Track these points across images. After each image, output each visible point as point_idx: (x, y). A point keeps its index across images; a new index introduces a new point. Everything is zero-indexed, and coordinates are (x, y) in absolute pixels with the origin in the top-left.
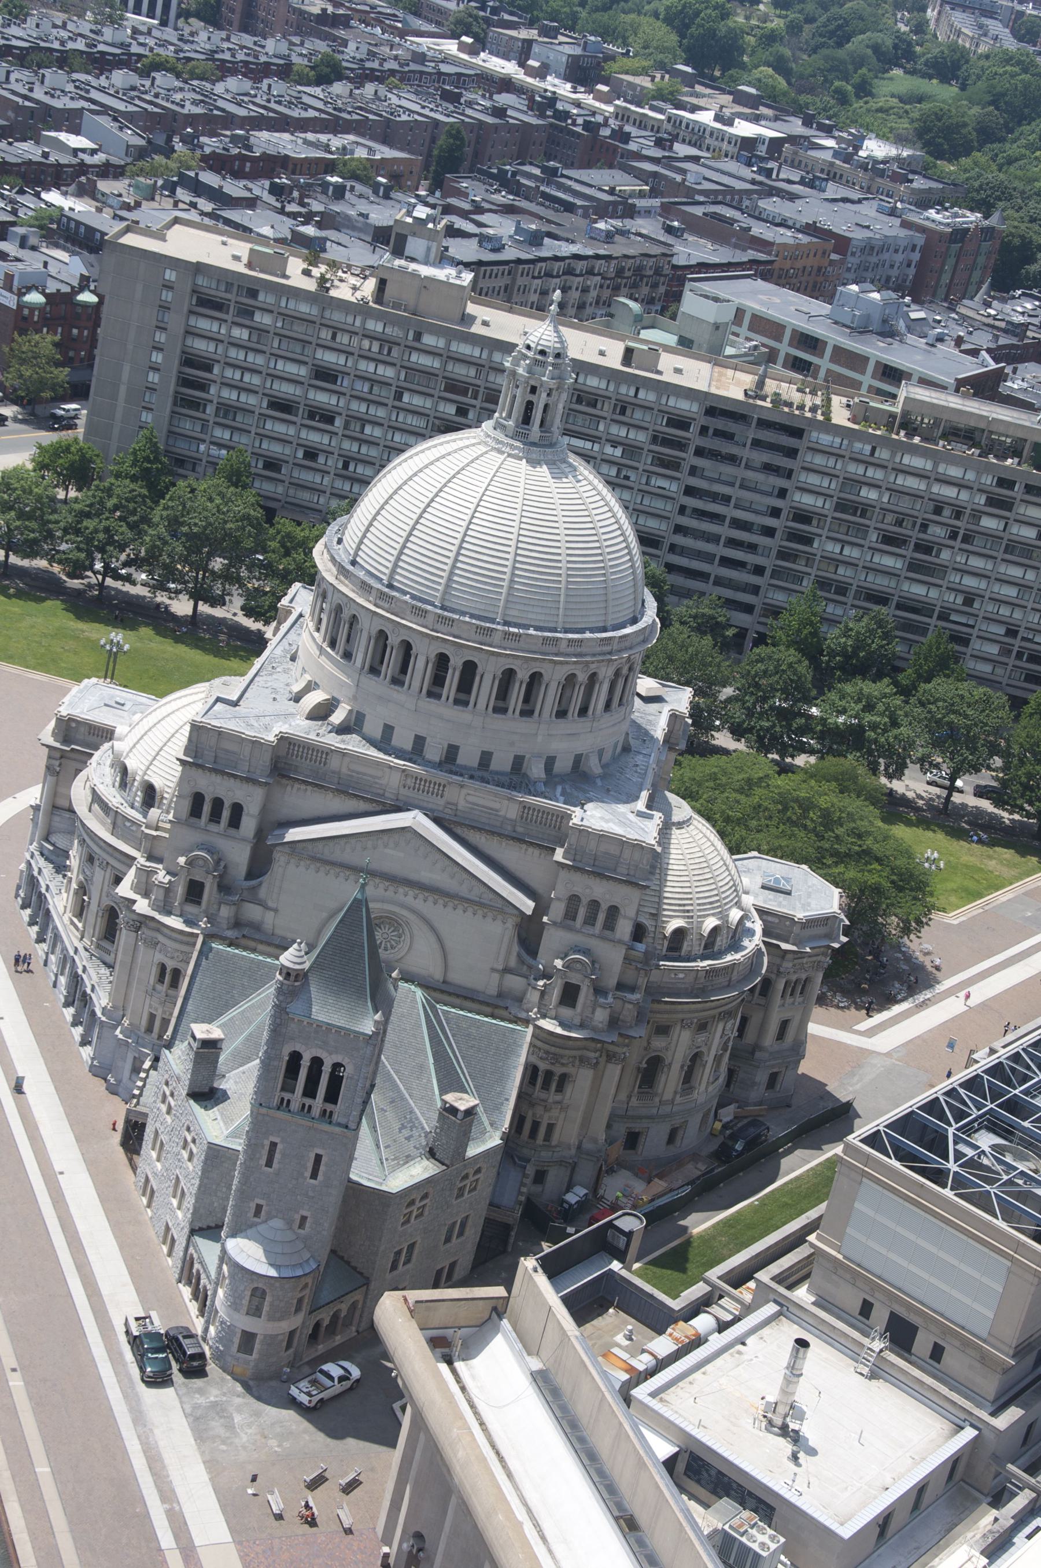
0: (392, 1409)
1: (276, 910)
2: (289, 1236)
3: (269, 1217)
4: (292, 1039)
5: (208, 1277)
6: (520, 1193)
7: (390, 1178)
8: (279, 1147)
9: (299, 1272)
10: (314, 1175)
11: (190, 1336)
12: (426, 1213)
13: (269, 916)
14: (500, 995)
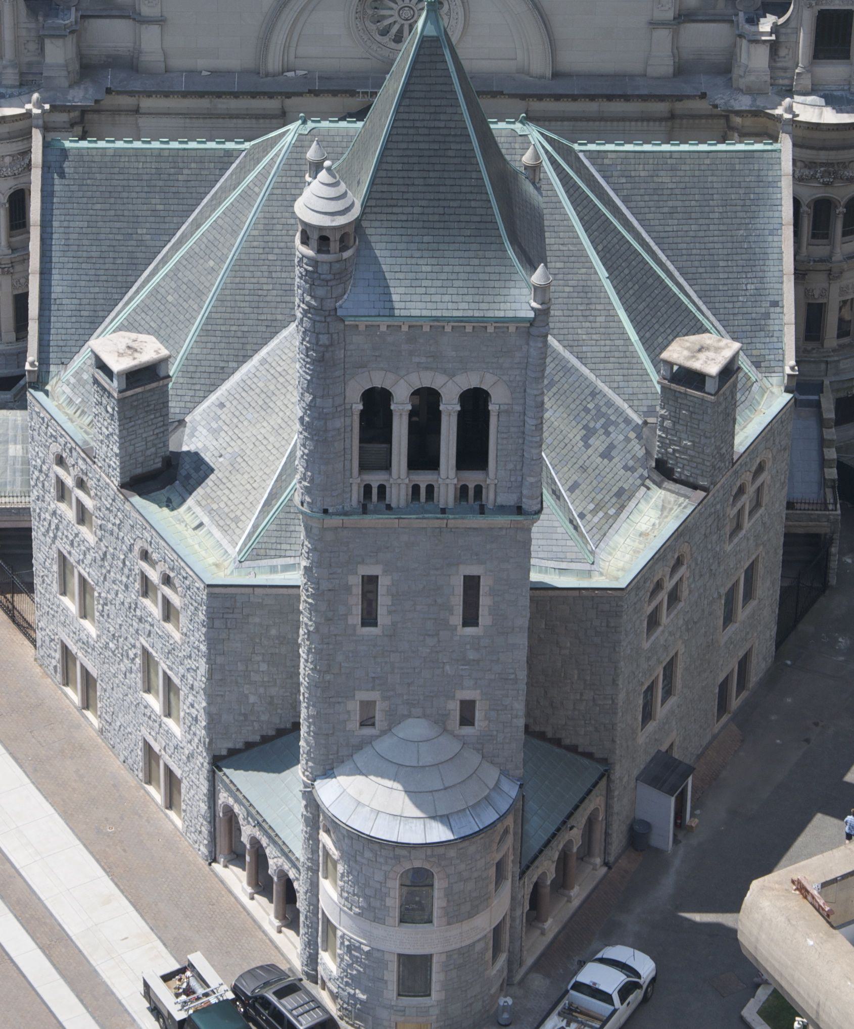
0: (742, 1020)
1: (160, 21)
2: (451, 747)
3: (394, 720)
4: (363, 366)
5: (286, 853)
6: (823, 463)
7: (602, 555)
8: (384, 583)
9: (490, 816)
10: (470, 619)
11: (291, 989)
12: (685, 593)
13: (150, 39)
14: (681, 70)
